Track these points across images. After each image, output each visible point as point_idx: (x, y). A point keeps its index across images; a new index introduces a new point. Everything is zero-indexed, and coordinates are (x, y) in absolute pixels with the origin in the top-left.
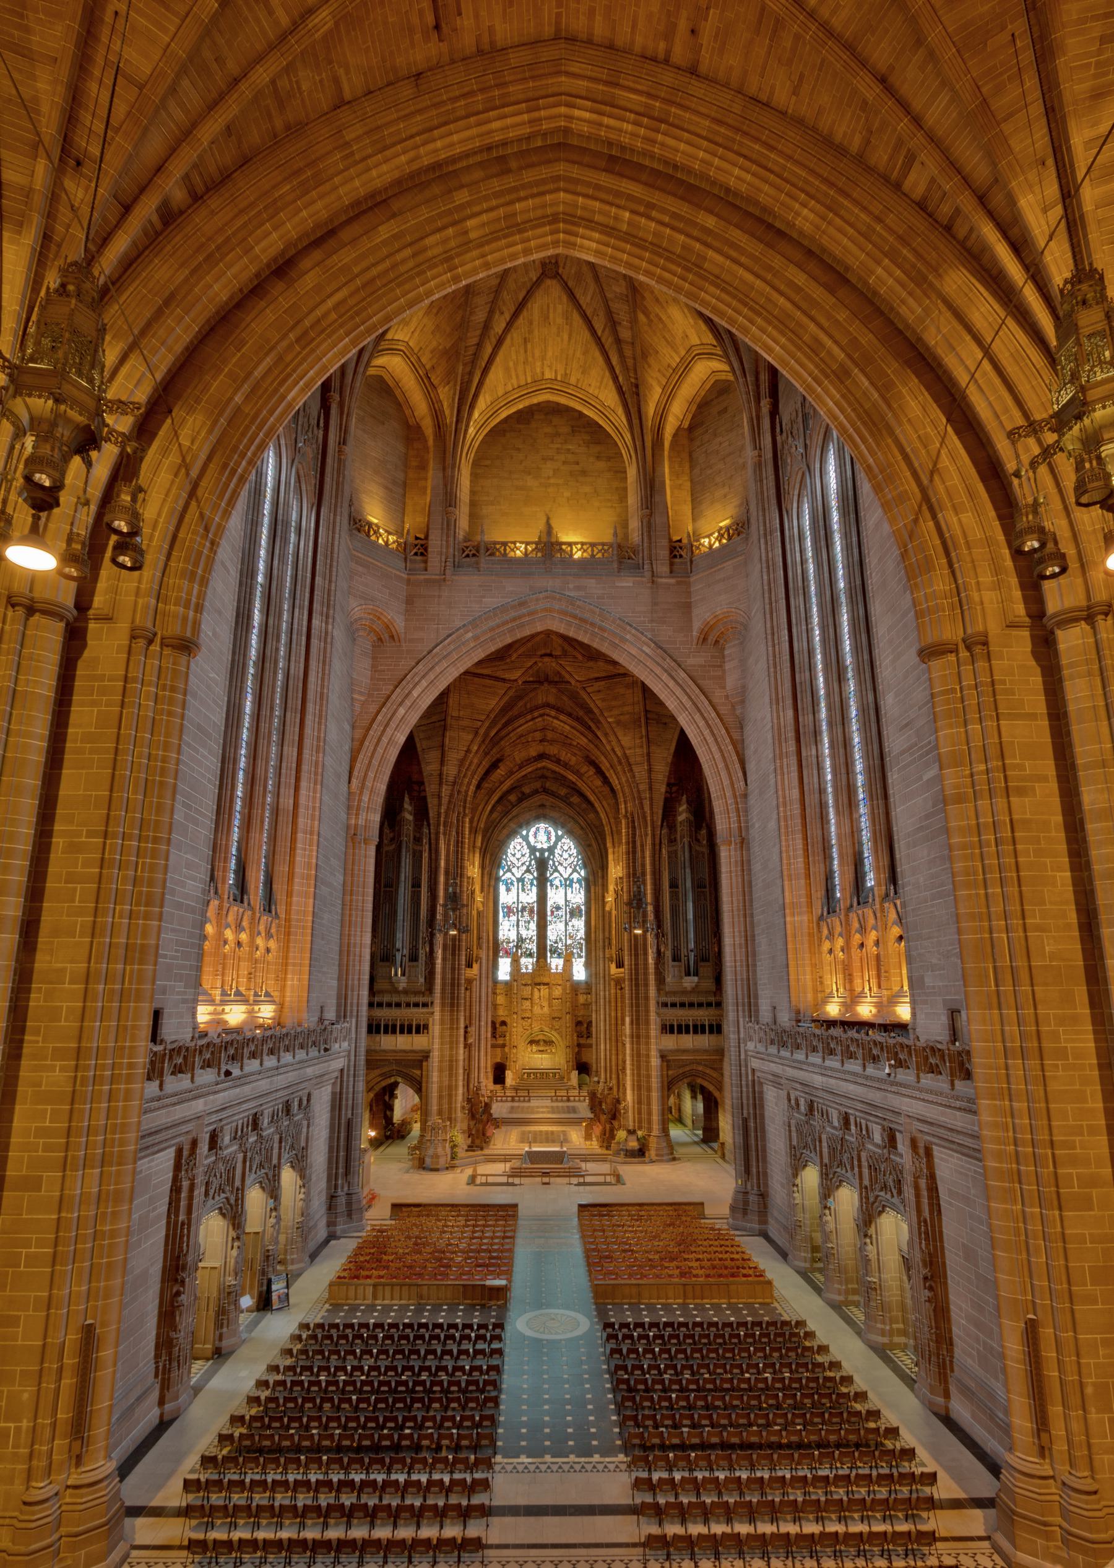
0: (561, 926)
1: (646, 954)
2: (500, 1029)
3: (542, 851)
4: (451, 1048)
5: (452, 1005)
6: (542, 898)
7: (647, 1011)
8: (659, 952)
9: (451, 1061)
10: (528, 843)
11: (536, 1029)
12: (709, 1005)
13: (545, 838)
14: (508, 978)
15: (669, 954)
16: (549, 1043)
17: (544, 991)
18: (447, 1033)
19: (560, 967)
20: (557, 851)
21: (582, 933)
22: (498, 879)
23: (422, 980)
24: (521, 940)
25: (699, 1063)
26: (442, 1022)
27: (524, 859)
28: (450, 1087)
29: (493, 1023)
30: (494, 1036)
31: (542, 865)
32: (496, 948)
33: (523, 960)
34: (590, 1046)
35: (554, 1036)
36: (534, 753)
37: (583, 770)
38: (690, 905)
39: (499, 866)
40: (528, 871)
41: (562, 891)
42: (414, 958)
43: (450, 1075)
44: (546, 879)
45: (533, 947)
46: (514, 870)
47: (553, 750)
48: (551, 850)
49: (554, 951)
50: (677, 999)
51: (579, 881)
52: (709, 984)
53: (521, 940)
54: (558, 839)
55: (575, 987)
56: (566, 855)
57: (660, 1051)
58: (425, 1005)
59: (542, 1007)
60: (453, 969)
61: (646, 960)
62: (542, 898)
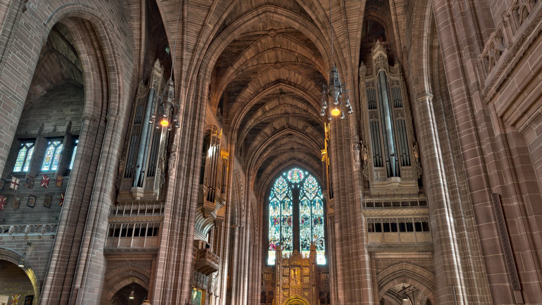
0: (309, 230)
3: (296, 184)
6: (296, 212)
10: (287, 180)
11: (292, 297)
12: (414, 204)
13: (298, 176)
15: (372, 161)
18: (176, 237)
19: (308, 256)
21: (322, 234)
22: (269, 202)
23: (158, 191)
24: (282, 239)
25: (408, 262)
29: (263, 294)
33: (284, 252)
36: (273, 79)
37: (307, 87)
38: (389, 119)
39: (268, 194)
40: (287, 196)
41: (308, 208)
42: (151, 174)
44: (299, 201)
45: (291, 243)
47: (284, 73)
48: (302, 184)
49: (303, 247)
50: (382, 200)
52: (413, 185)
54: (306, 177)
55: (319, 269)
58: (157, 211)
60: (187, 186)
61: (351, 170)
62: (296, 212)
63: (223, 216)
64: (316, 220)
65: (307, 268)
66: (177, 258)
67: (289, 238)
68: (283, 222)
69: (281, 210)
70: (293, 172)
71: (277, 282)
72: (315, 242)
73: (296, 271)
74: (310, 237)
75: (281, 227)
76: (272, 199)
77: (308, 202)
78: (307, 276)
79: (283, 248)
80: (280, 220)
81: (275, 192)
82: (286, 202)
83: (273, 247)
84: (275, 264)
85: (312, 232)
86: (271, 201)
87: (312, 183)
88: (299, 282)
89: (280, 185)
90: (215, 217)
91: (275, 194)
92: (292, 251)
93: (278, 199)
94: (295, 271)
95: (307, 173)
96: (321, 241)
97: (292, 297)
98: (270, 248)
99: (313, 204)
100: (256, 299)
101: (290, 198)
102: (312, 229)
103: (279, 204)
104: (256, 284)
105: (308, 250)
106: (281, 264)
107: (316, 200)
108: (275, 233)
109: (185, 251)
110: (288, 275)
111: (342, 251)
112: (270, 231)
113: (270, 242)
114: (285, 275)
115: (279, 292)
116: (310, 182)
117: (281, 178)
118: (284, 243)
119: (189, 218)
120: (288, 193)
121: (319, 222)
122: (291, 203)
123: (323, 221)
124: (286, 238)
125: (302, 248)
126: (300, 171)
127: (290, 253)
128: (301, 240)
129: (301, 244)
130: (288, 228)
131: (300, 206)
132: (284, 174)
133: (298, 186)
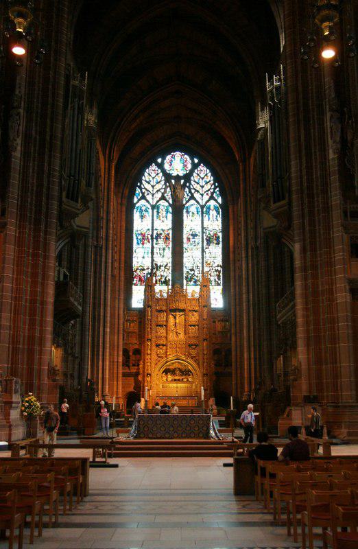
0: (198, 253)
1: (324, 150)
2: (133, 358)
3: (178, 178)
4: (34, 283)
5: (37, 222)
7: (328, 228)
8: (344, 141)
9: (33, 301)
10: (164, 171)
11: (171, 357)
14: (141, 306)
16: (186, 372)
17: (180, 318)
19: (197, 295)
20: (195, 177)
21: (219, 261)
24: (155, 267)
26: (20, 242)
27: (158, 187)
28: (31, 340)
29: (126, 352)
30: (126, 363)
31: (178, 186)
32: (129, 275)
33: (158, 288)
34: (230, 374)
35: (190, 364)
39: (133, 193)
40: (163, 198)
41: (198, 218)
43: (32, 323)
44: (183, 206)
46: (149, 197)
48: (187, 177)
49: (189, 279)
51: (215, 208)
53: (158, 267)
54: (195, 166)
55: (213, 314)
56: (202, 183)
57: (351, 282)
59: (178, 334)
63: (87, 226)
64: (209, 238)
65: (195, 313)
66: (31, 296)
67: (167, 265)
68: (157, 241)
69: (153, 220)
70: (173, 157)
71: (148, 335)
72: (207, 272)
73: (177, 317)
74: (200, 265)
75: (153, 248)
76: (138, 202)
77: (197, 209)
78: (194, 326)
79: (156, 281)
80: (152, 236)
81: (143, 190)
82: (161, 207)
83: (140, 280)
84: (144, 305)
85: (203, 258)
86: (137, 205)
87: (204, 179)
88: (182, 334)
89: (151, 179)
90: (75, 227)
91: (143, 194)
92: (170, 287)
93: (148, 201)
94: (175, 318)
95: (196, 161)
96: (216, 271)
97: (171, 357)
98: (135, 282)
99: (206, 211)
100: (116, 360)
101: (168, 201)
102: (203, 251)
103: (150, 211)
104: (116, 337)
105: (196, 285)
106: (153, 307)
107: (210, 205)
108: (143, 257)
109: (43, 284)
110: (165, 323)
111: (305, 287)
112: (134, 255)
113: (135, 271)
114: (159, 323)
115: (151, 350)
116: (202, 175)
117: (154, 167)
118: (158, 273)
119: (46, 227)
120: (165, 192)
121: (215, 241)
122: (170, 209)
123: (221, 240)
124: (161, 266)
125: (187, 281)
126: (186, 156)
127: (168, 290)
128: (185, 270)
129: (184, 275)
130: (164, 249)
131: (185, 214)
132: (159, 160)
133: (182, 181)
